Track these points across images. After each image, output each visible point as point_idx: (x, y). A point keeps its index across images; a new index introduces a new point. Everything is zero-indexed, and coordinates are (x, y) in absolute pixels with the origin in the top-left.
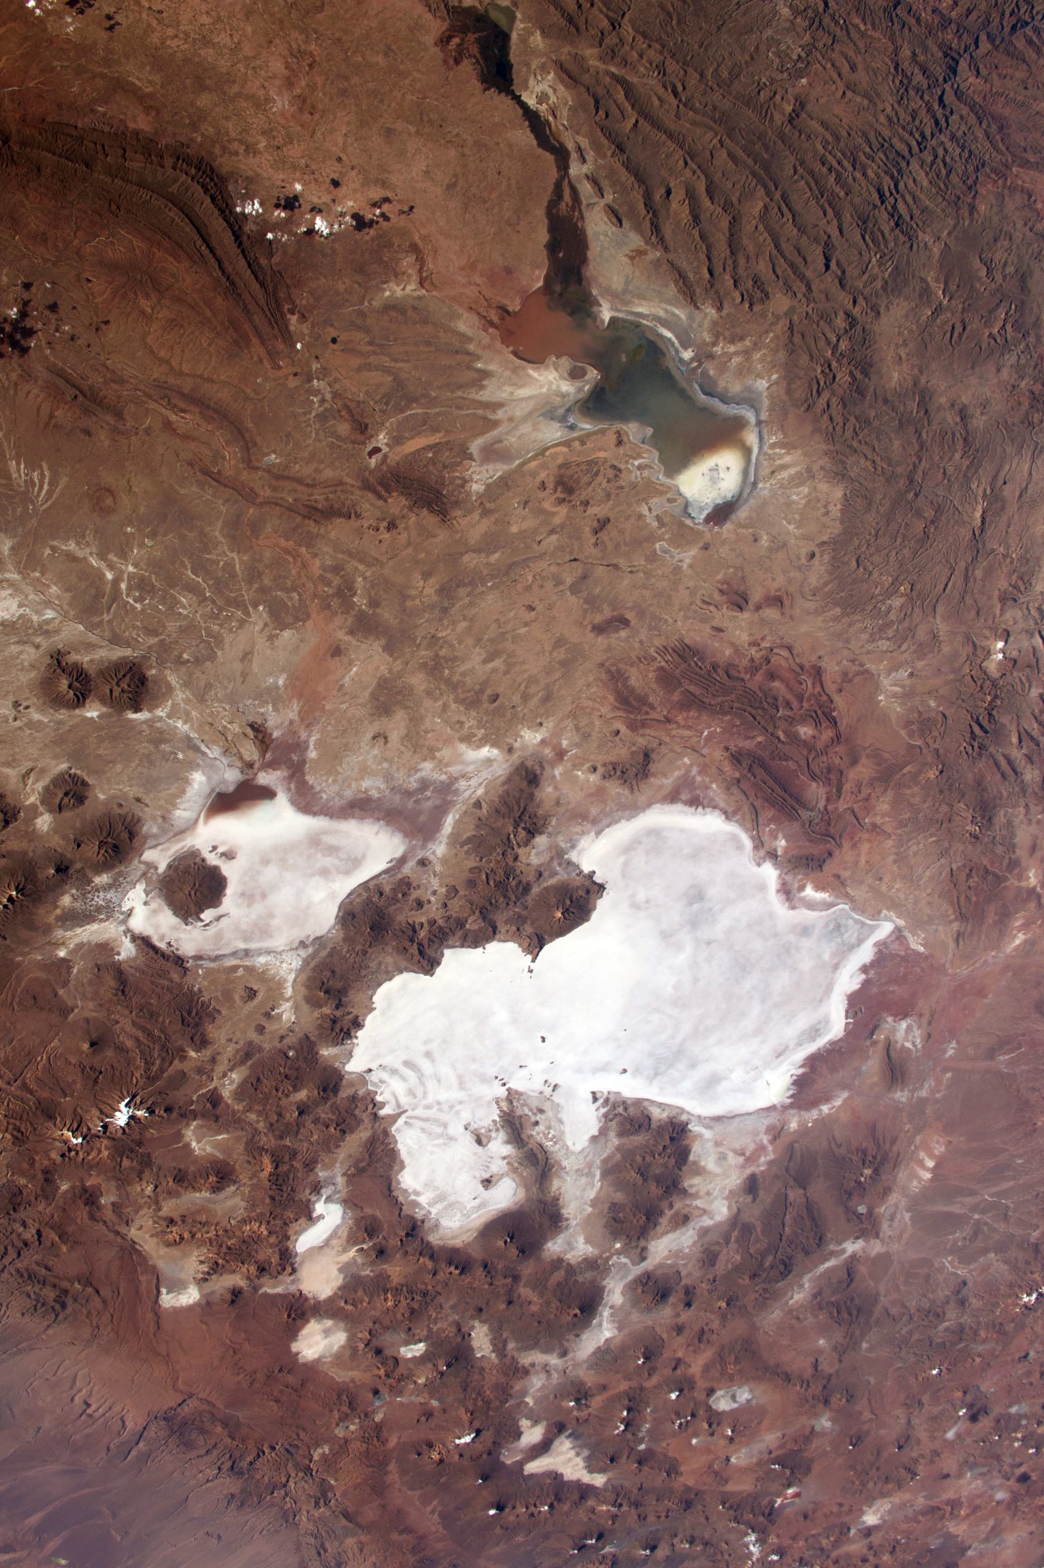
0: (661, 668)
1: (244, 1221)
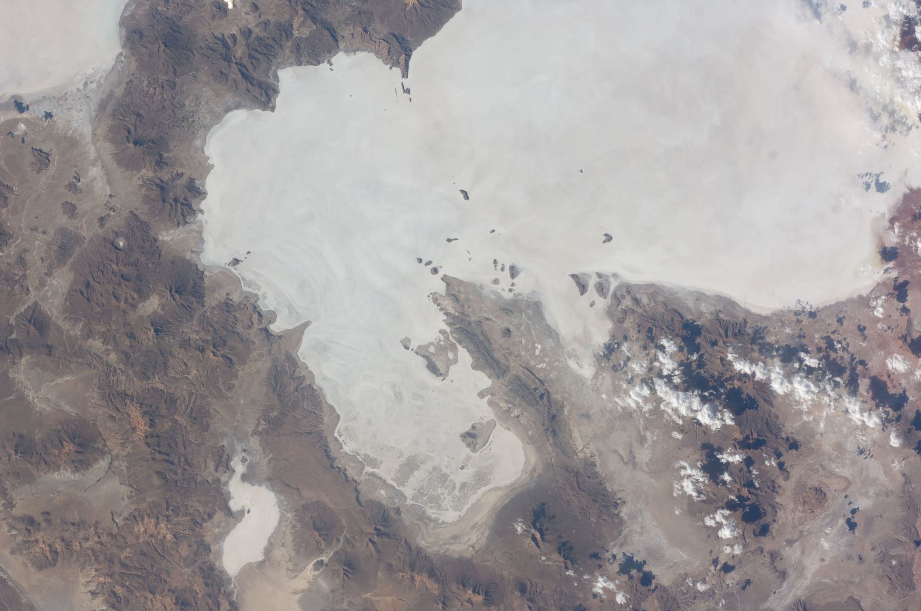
1: (134, 518)
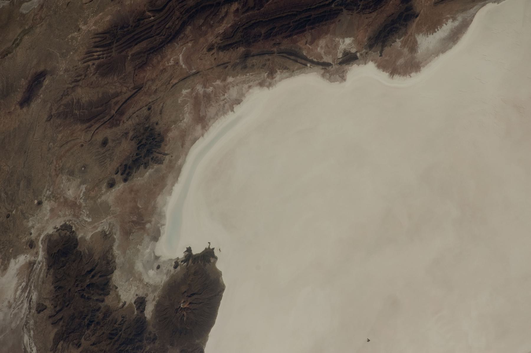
0: (99, 67)
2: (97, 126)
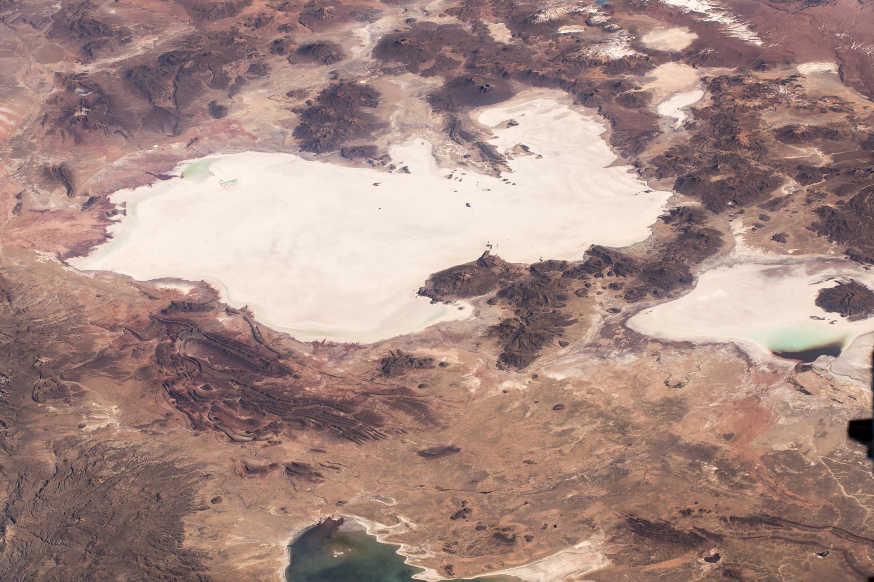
0: (378, 426)
2: (418, 398)
